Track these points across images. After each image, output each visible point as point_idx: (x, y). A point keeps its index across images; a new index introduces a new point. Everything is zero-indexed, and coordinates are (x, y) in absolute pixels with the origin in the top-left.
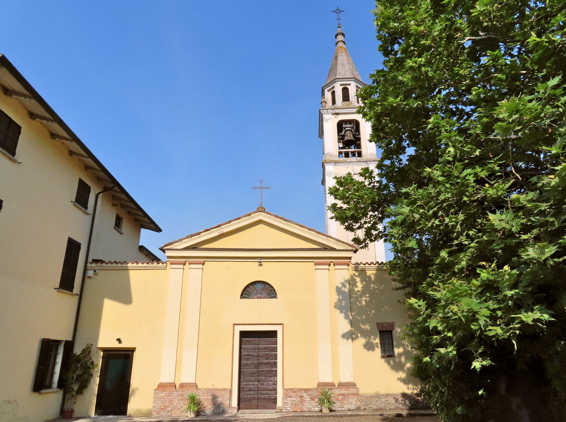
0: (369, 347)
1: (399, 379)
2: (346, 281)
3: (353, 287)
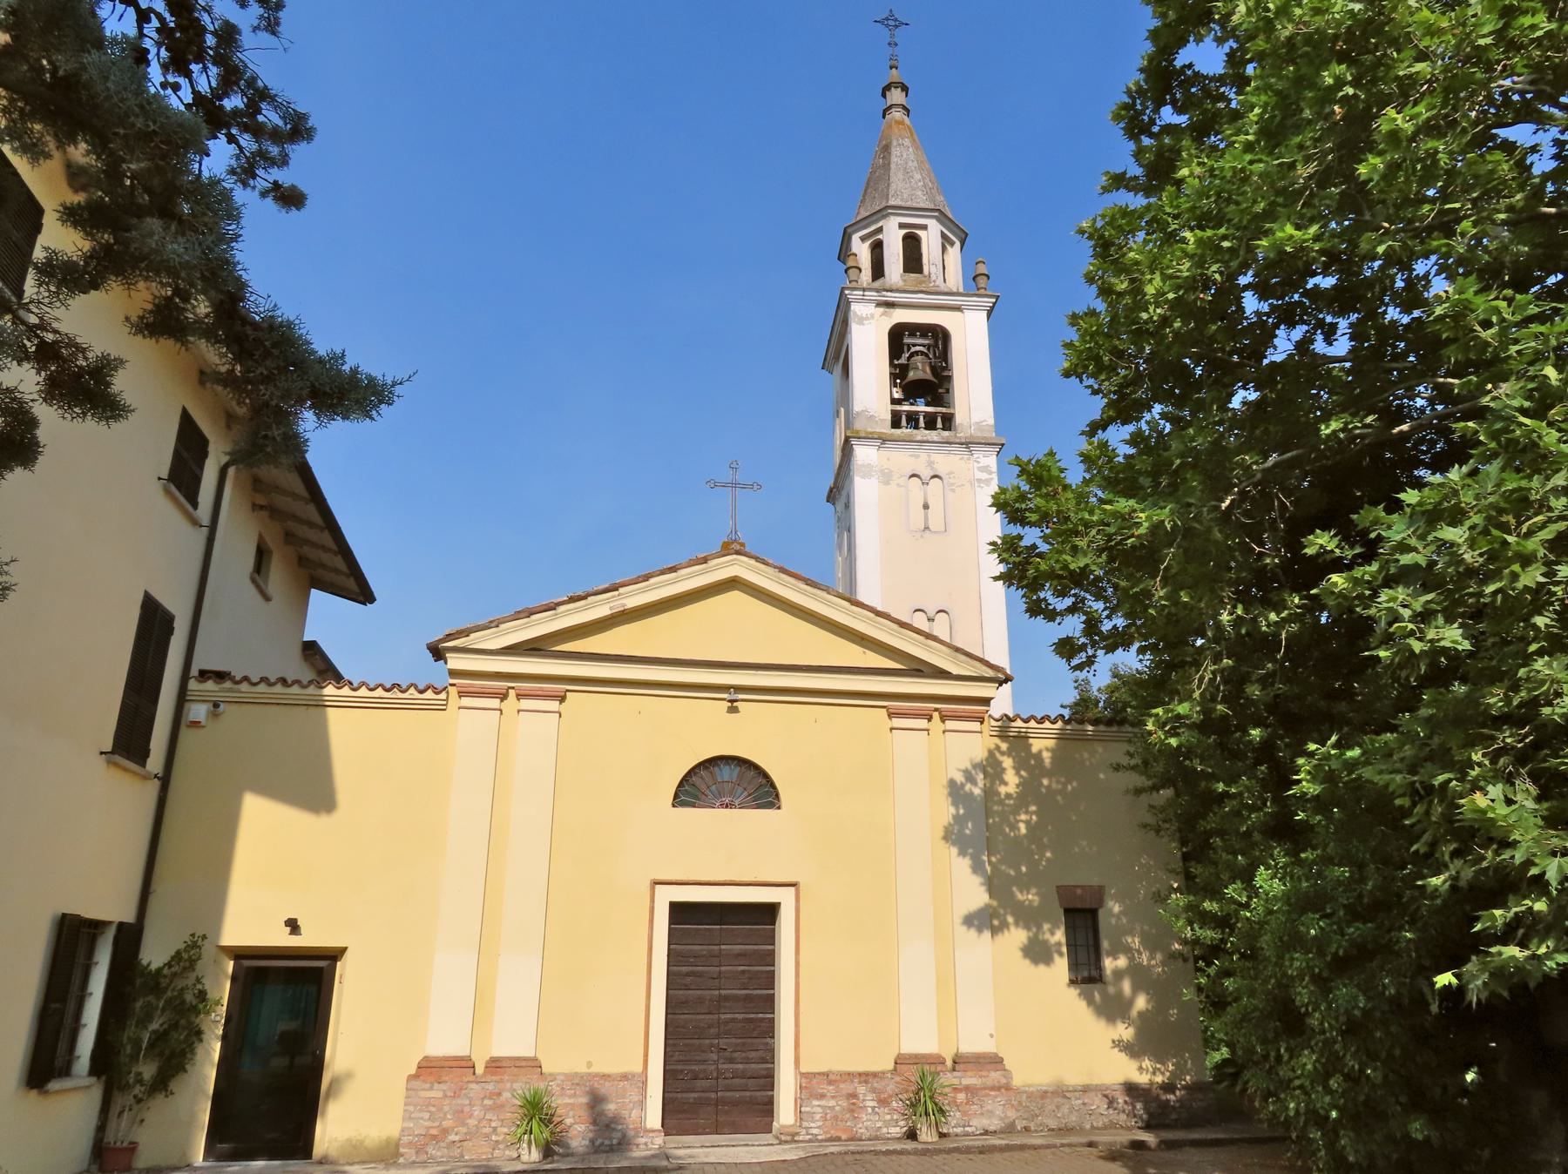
0: (1037, 953)
1: (1119, 1044)
2: (975, 766)
3: (993, 783)
